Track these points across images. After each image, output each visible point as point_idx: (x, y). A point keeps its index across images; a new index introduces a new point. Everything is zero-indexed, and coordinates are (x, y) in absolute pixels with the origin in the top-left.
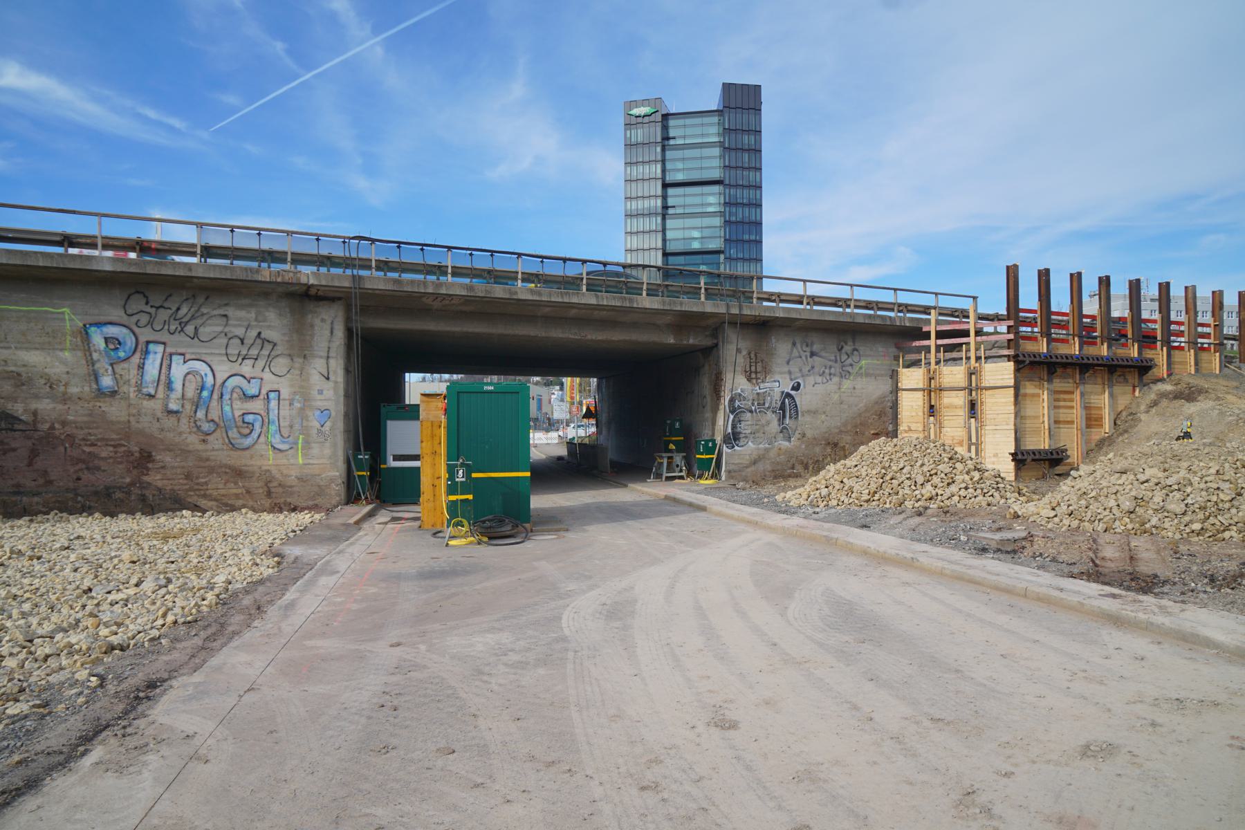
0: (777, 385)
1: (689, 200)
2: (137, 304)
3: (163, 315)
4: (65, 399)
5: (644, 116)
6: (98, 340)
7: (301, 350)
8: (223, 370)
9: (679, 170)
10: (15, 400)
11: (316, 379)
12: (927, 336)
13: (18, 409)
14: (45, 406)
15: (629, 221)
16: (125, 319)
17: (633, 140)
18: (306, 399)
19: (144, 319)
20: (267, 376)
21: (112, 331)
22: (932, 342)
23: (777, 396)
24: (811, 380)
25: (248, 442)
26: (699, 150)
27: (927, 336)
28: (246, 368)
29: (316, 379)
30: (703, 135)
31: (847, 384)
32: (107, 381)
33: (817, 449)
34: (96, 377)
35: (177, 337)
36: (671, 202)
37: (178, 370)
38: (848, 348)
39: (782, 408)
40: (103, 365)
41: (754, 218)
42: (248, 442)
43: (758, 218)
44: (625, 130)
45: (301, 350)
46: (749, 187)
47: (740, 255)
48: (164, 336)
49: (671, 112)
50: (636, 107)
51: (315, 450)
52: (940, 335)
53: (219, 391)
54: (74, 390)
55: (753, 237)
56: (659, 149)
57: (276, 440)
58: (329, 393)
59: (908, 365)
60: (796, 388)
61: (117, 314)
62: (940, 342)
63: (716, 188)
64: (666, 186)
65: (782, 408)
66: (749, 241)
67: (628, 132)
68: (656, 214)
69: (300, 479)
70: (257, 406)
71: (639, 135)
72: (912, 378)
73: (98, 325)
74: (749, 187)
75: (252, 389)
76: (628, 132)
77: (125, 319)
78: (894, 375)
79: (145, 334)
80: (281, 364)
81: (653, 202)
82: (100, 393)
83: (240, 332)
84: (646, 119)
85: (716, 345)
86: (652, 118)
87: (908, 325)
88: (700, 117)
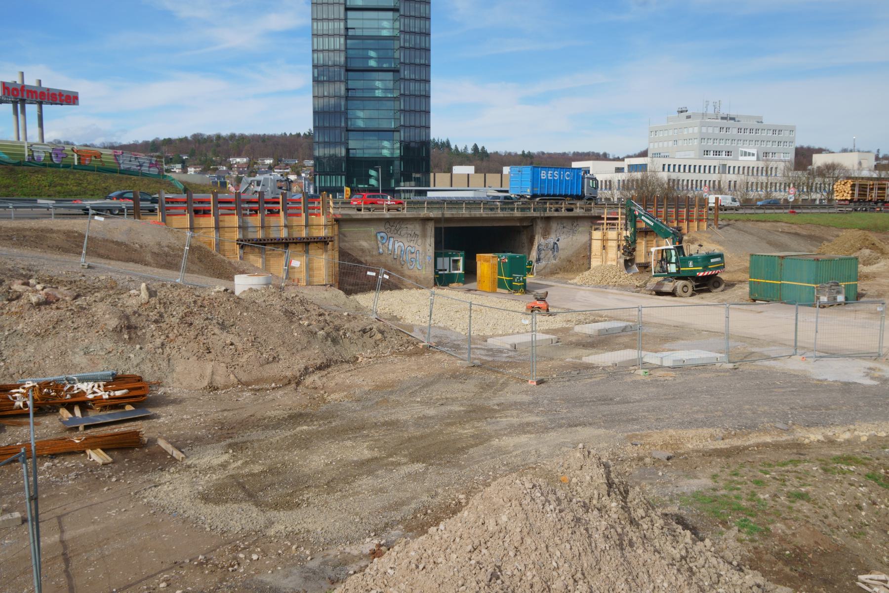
0: (552, 239)
1: (367, 24)
2: (387, 226)
3: (393, 228)
4: (372, 256)
6: (379, 238)
7: (424, 236)
8: (407, 244)
10: (361, 256)
11: (428, 246)
12: (603, 219)
13: (363, 260)
14: (368, 258)
15: (315, 40)
16: (385, 231)
18: (425, 253)
19: (389, 230)
20: (416, 246)
21: (382, 234)
22: (605, 222)
23: (552, 244)
24: (563, 237)
25: (412, 267)
27: (603, 219)
28: (412, 244)
29: (428, 246)
31: (574, 238)
32: (381, 250)
33: (564, 263)
34: (379, 248)
35: (396, 235)
37: (396, 245)
38: (575, 224)
39: (554, 248)
40: (380, 245)
41: (423, 45)
42: (412, 267)
43: (427, 45)
45: (424, 236)
46: (420, 18)
47: (413, 77)
48: (393, 235)
51: (427, 269)
52: (608, 219)
53: (405, 252)
54: (374, 253)
55: (423, 62)
57: (418, 266)
58: (431, 251)
59: (595, 229)
60: (558, 241)
61: (383, 229)
62: (608, 222)
63: (390, 14)
65: (554, 248)
66: (420, 65)
68: (340, 35)
69: (424, 278)
70: (414, 256)
72: (597, 235)
73: (379, 233)
74: (420, 18)
75: (413, 251)
77: (385, 231)
78: (590, 234)
79: (389, 235)
80: (420, 241)
81: (337, 24)
82: (380, 254)
83: (410, 232)
85: (532, 225)
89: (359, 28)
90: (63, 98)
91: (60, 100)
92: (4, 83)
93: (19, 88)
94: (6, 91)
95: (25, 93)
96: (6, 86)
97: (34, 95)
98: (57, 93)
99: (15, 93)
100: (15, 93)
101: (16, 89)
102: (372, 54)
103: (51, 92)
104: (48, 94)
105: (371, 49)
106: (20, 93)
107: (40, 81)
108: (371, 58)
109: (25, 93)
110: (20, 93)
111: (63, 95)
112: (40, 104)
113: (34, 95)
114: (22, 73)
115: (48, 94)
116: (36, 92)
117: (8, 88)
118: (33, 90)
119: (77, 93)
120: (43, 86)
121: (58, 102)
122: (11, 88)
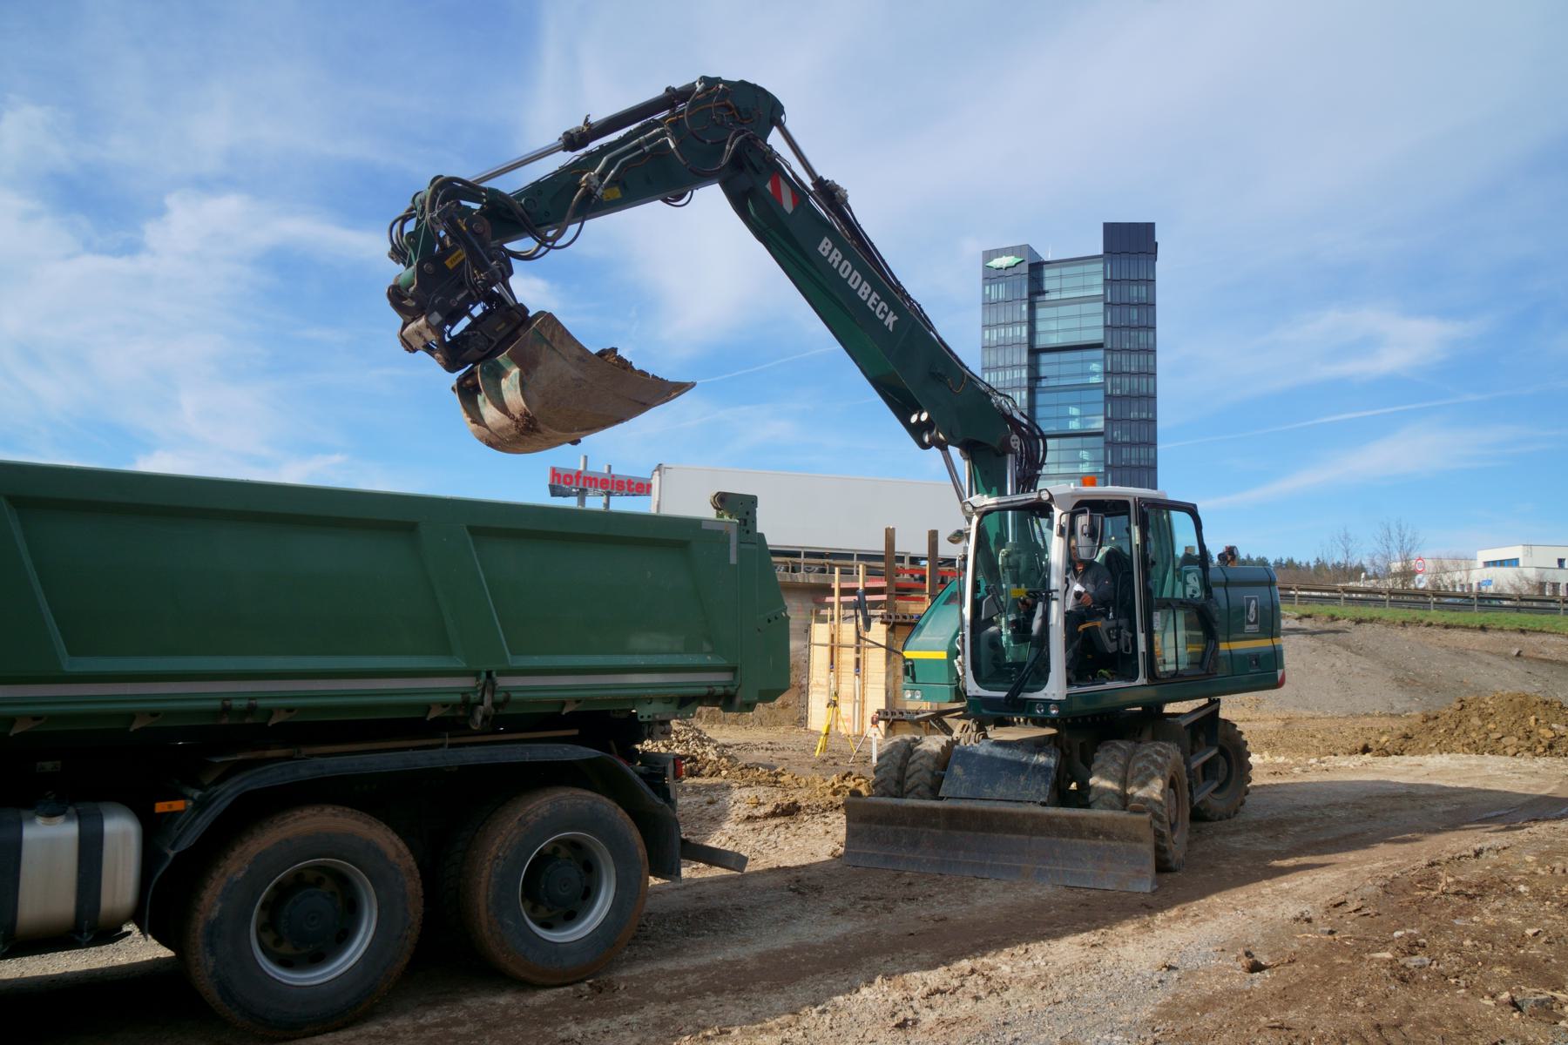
1: (1065, 369)
5: (1006, 268)
9: (1052, 332)
17: (993, 297)
22: (835, 599)
26: (1078, 306)
30: (1084, 287)
36: (1043, 371)
41: (1145, 390)
43: (1151, 390)
44: (984, 285)
46: (1139, 351)
47: (1126, 439)
49: (1046, 260)
50: (997, 257)
55: (1144, 415)
56: (1025, 307)
62: (844, 599)
63: (1100, 353)
64: (1034, 352)
66: (1140, 420)
67: (987, 288)
71: (999, 292)
74: (1139, 351)
76: (987, 288)
84: (1009, 272)
86: (1016, 270)
87: (813, 582)
88: (1057, 267)
89: (1052, 377)
90: (633, 486)
93: (574, 474)
94: (556, 478)
95: (581, 481)
96: (557, 472)
97: (593, 482)
98: (626, 481)
99: (568, 480)
100: (568, 480)
101: (571, 477)
102: (1074, 411)
103: (616, 480)
104: (613, 481)
105: (1074, 405)
106: (574, 480)
107: (610, 467)
108: (1073, 417)
109: (581, 481)
110: (574, 480)
111: (632, 483)
112: (609, 494)
113: (593, 482)
115: (613, 481)
116: (596, 479)
117: (559, 476)
118: (593, 477)
120: (613, 472)
121: (626, 491)
122: (562, 475)
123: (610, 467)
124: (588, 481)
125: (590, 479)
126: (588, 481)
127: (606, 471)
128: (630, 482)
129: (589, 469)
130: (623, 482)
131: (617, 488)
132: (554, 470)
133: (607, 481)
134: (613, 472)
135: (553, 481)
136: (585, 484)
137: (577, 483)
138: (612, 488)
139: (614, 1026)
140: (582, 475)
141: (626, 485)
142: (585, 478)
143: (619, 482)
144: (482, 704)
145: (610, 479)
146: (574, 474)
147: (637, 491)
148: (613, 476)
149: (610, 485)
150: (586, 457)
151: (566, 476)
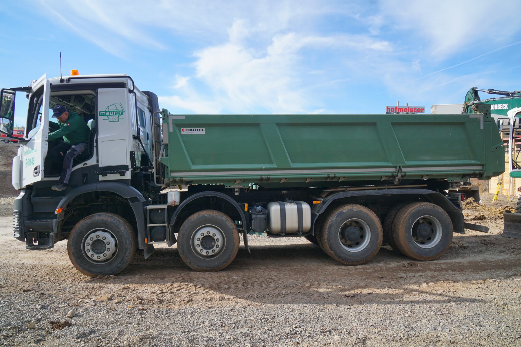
90: (416, 110)
91: (415, 111)
92: (387, 107)
93: (394, 108)
94: (388, 110)
95: (397, 110)
96: (388, 108)
97: (402, 110)
98: (413, 108)
99: (393, 110)
100: (393, 110)
104: (409, 109)
106: (395, 110)
107: (407, 104)
109: (397, 110)
110: (395, 110)
111: (416, 109)
113: (402, 110)
114: (399, 102)
116: (402, 109)
117: (389, 109)
119: (424, 107)
120: (409, 106)
123: (407, 104)
124: (400, 110)
125: (400, 109)
126: (400, 110)
127: (406, 106)
128: (415, 109)
129: (400, 105)
130: (412, 109)
131: (411, 111)
132: (387, 107)
133: (407, 109)
134: (409, 106)
135: (387, 111)
136: (398, 111)
137: (396, 111)
138: (409, 111)
139: (416, 275)
140: (398, 108)
141: (414, 110)
142: (399, 109)
143: (411, 109)
144: (398, 176)
145: (408, 108)
146: (394, 108)
147: (418, 111)
148: (409, 107)
149: (408, 110)
150: (399, 102)
151: (392, 109)
